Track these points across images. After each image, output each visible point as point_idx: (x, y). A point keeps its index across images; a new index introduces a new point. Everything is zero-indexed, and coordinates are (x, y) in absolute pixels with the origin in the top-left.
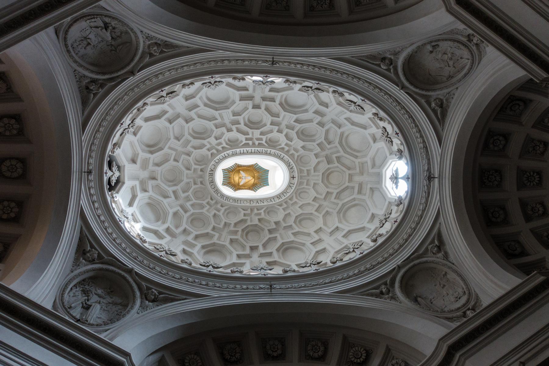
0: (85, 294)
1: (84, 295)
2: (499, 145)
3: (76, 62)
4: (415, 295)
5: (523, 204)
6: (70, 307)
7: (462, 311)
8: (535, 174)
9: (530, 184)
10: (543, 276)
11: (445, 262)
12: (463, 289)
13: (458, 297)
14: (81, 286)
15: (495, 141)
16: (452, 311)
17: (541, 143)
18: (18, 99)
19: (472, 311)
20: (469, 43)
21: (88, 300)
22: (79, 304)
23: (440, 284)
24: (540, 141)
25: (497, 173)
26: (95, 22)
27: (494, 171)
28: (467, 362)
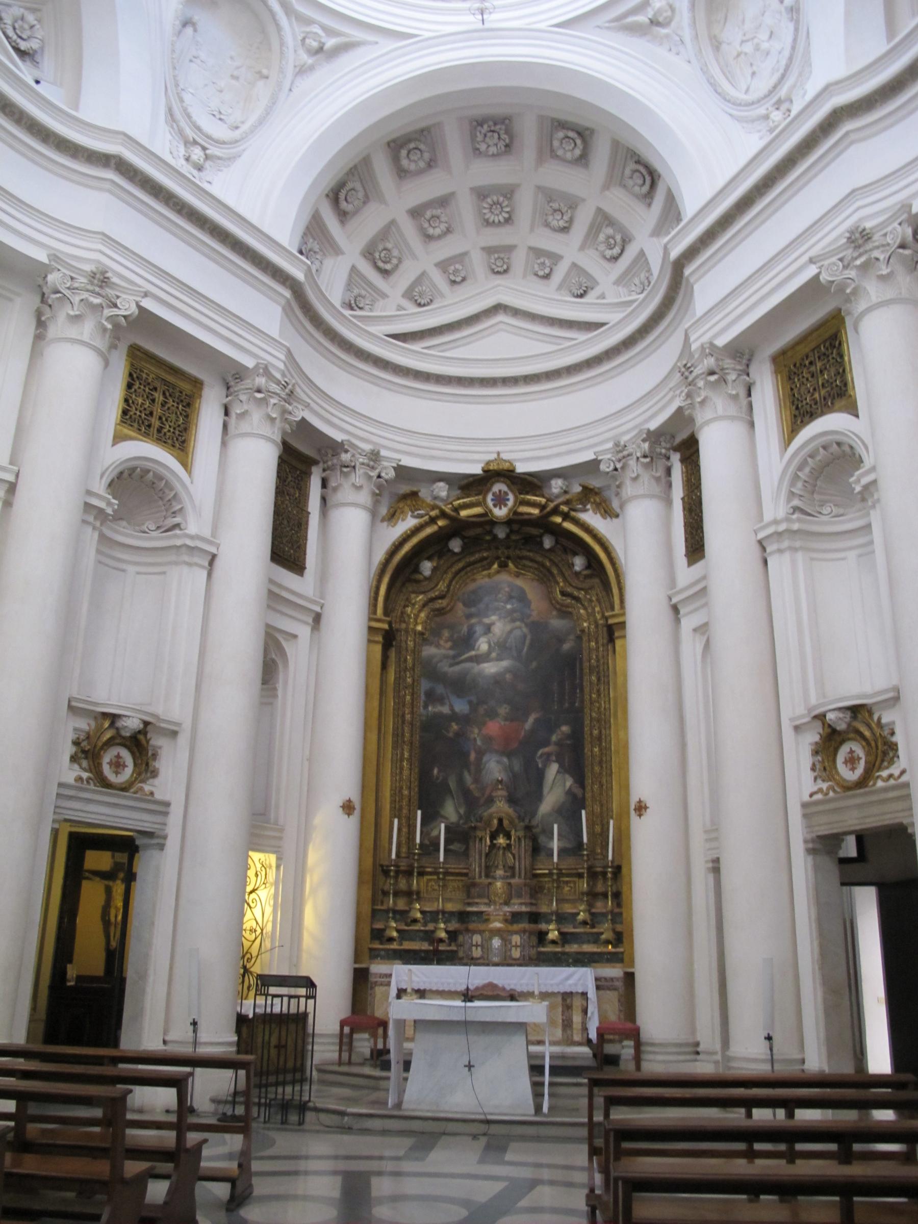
2: (564, 149)
4: (196, 18)
5: (443, 201)
7: (196, 137)
8: (506, 216)
9: (485, 208)
10: (306, 276)
11: (290, 71)
12: (243, 123)
13: (222, 117)
15: (571, 141)
16: (189, 116)
17: (567, 222)
19: (204, 157)
20: (775, 99)
23: (238, 68)
24: (571, 221)
25: (503, 148)
27: (507, 141)
28: (107, 195)
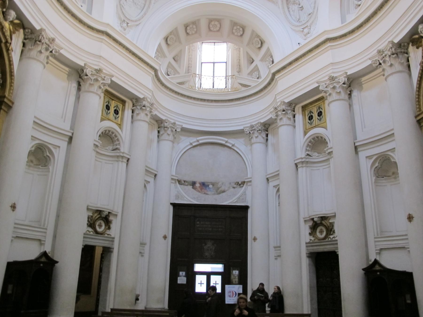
0: (295, 3)
1: (296, 4)
3: (149, 7)
6: (299, 20)
14: (290, 4)
18: (176, 29)
21: (299, 4)
22: (299, 12)
26: (124, 3)
